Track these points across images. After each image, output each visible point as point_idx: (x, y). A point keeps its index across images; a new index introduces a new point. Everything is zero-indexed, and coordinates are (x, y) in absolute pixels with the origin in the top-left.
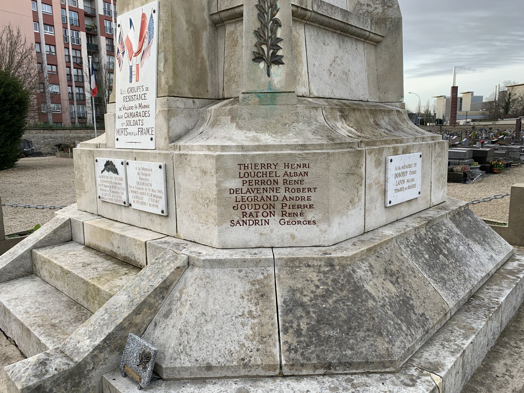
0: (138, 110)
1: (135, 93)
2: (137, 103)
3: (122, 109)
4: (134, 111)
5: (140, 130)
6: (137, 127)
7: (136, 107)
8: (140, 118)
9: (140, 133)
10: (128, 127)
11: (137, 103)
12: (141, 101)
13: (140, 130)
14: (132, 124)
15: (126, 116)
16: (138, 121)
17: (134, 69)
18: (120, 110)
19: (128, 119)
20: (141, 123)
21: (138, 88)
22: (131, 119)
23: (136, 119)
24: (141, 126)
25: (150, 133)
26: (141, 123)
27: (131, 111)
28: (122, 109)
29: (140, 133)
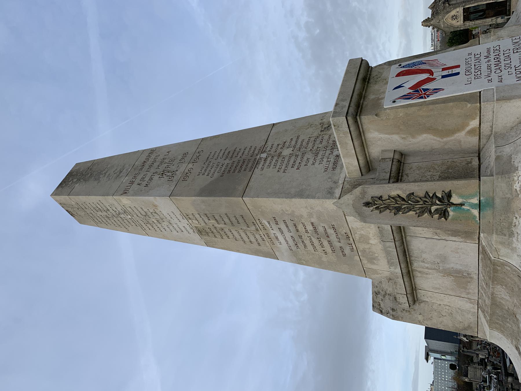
0: (492, 59)
1: (473, 67)
2: (483, 61)
3: (489, 78)
4: (493, 62)
5: (515, 51)
6: (512, 56)
7: (489, 61)
8: (501, 54)
9: (518, 50)
10: (513, 66)
11: (483, 61)
12: (482, 58)
13: (515, 51)
14: (509, 62)
15: (499, 71)
16: (505, 55)
17: (445, 73)
18: (490, 81)
19: (503, 68)
20: (508, 52)
21: (467, 63)
22: (503, 64)
23: (502, 58)
24: (511, 51)
25: (519, 40)
26: (508, 52)
27: (493, 66)
28: (489, 78)
29: (518, 50)
